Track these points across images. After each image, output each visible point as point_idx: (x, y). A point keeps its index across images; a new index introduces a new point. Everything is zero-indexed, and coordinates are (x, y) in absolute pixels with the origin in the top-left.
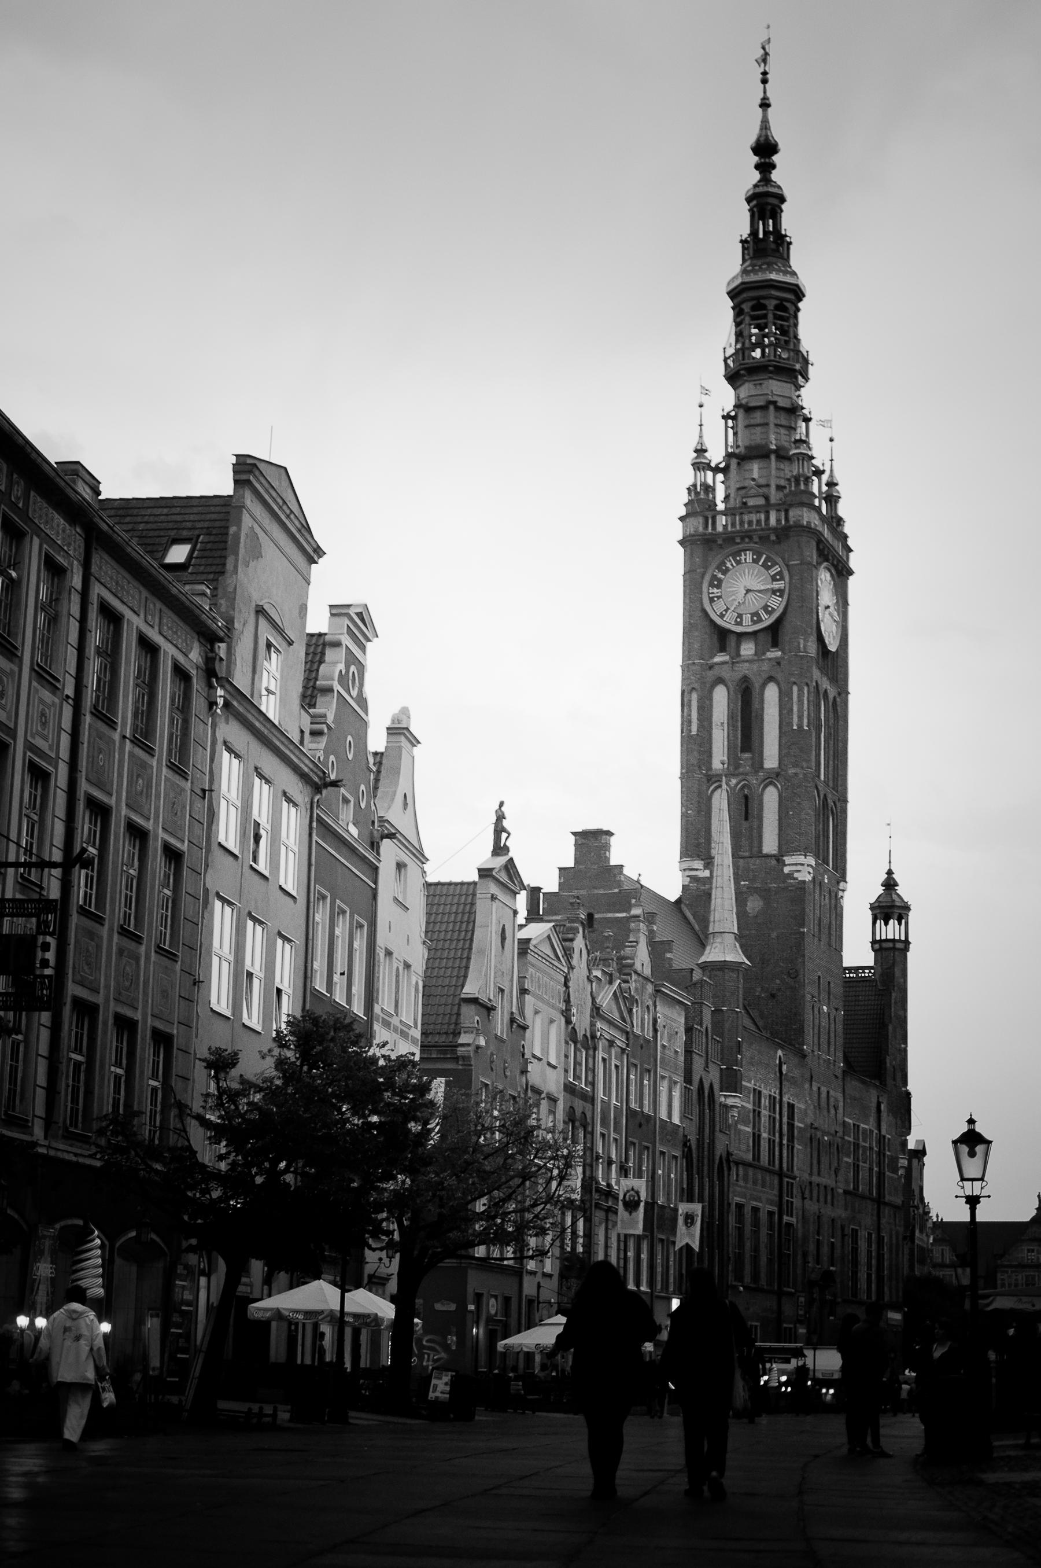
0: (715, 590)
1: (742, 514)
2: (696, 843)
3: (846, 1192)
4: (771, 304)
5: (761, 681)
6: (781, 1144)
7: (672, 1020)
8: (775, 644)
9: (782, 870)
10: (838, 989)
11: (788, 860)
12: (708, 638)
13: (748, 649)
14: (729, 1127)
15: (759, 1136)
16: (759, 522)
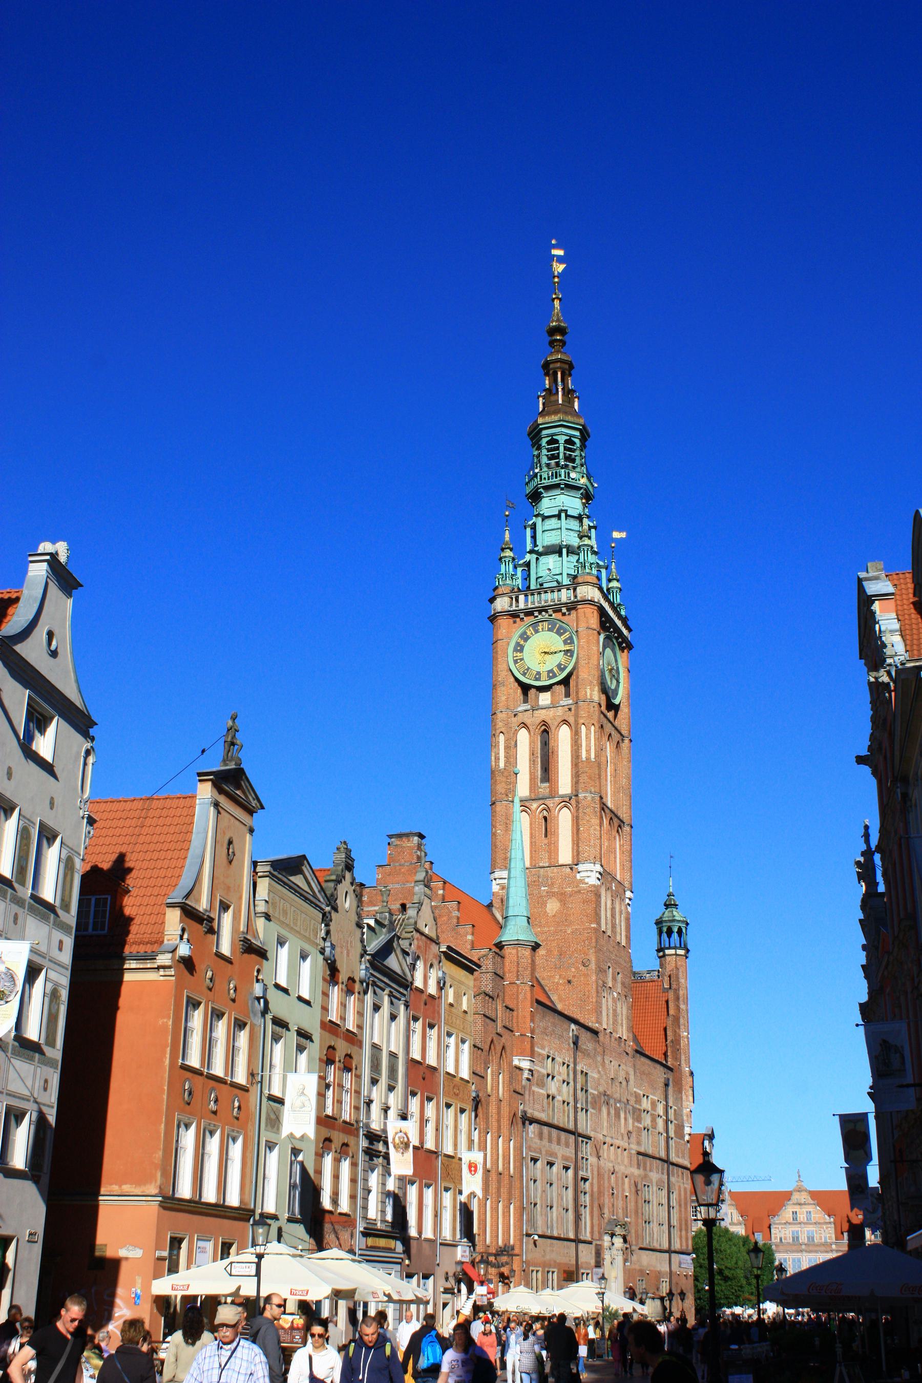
0: (519, 654)
1: (539, 593)
3: (639, 1153)
4: (562, 439)
5: (556, 724)
6: (576, 1108)
8: (567, 695)
9: (575, 877)
11: (581, 867)
13: (545, 699)
14: (524, 1087)
15: (553, 1098)
16: (553, 600)
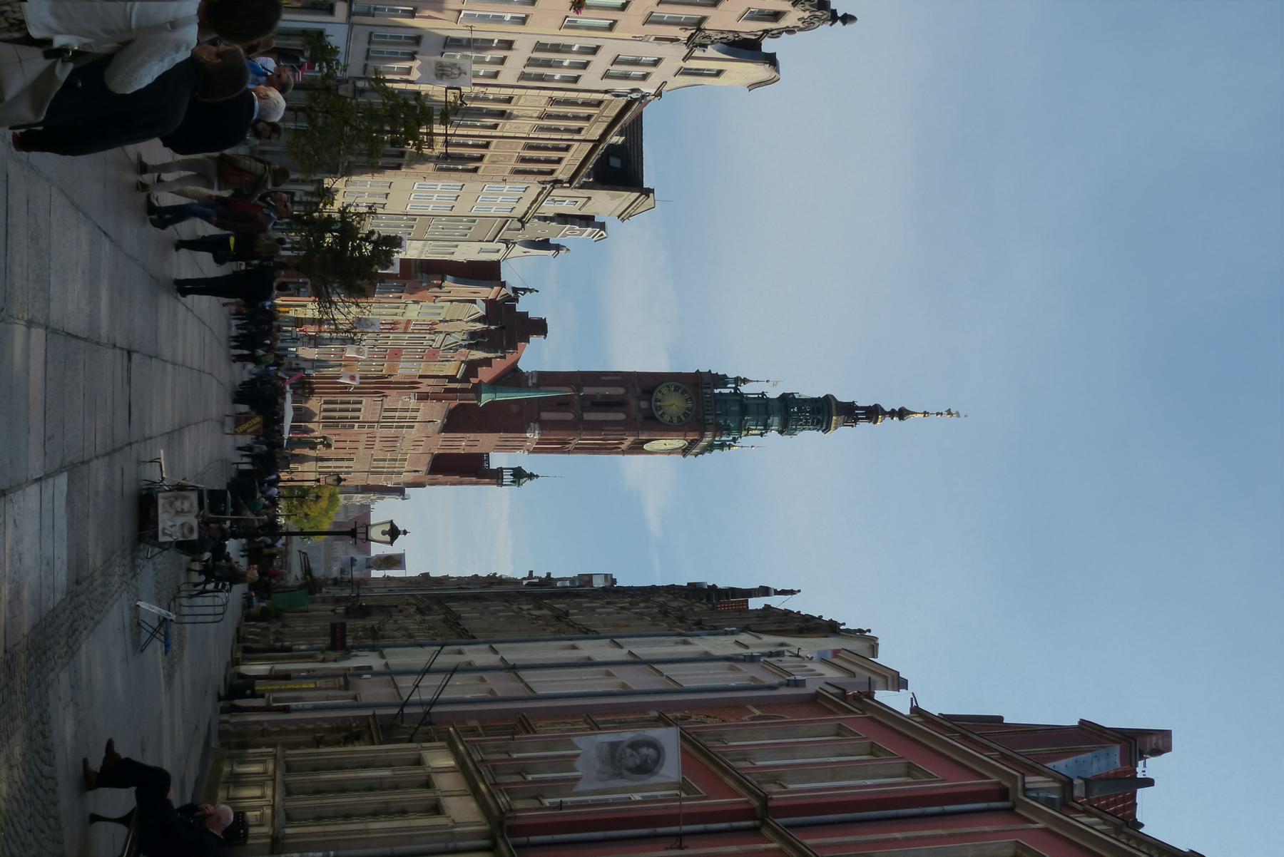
2: (546, 379)
7: (451, 369)
8: (646, 418)
10: (474, 450)
12: (648, 384)
13: (643, 404)
